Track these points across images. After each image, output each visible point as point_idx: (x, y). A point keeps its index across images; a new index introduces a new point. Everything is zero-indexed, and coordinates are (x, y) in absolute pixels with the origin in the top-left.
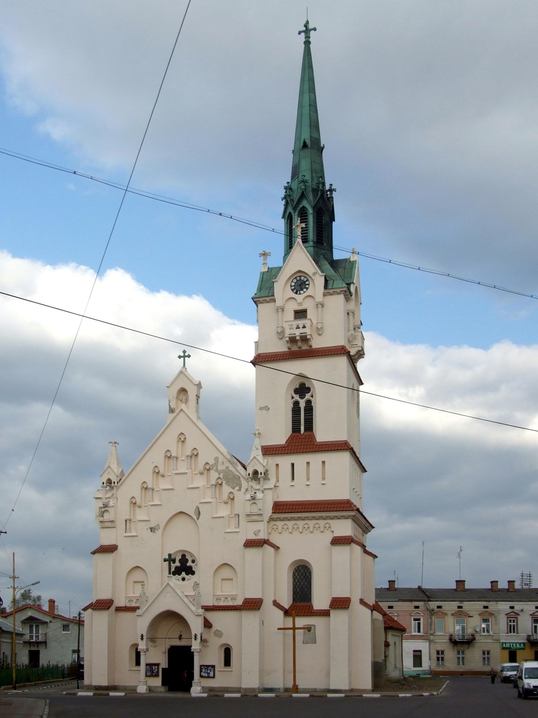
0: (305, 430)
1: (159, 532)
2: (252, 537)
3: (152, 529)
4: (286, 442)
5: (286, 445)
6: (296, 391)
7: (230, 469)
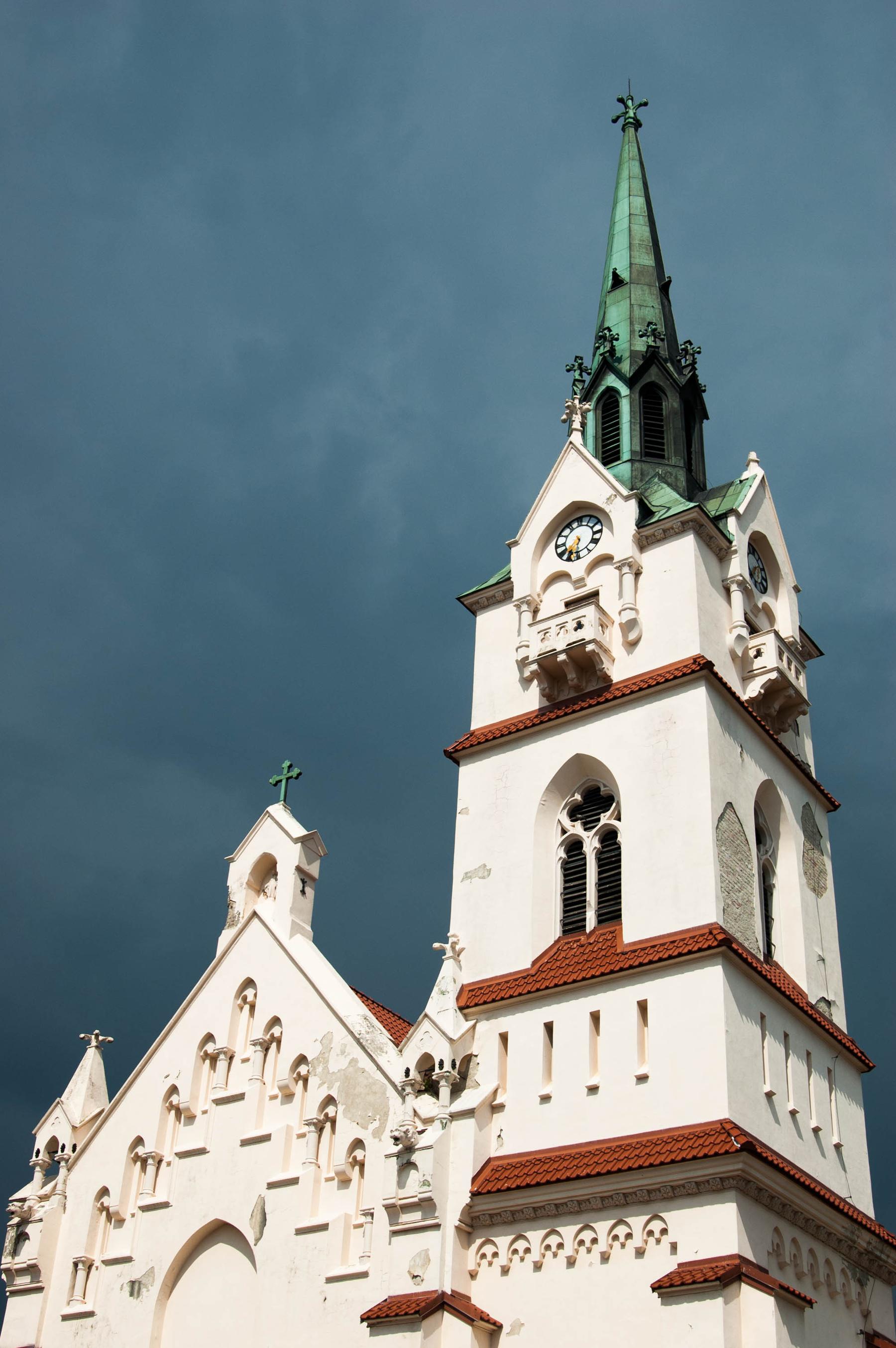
0: (600, 922)
1: (152, 1293)
2: (405, 1287)
3: (135, 1288)
4: (534, 963)
5: (533, 972)
6: (574, 813)
7: (361, 1065)
